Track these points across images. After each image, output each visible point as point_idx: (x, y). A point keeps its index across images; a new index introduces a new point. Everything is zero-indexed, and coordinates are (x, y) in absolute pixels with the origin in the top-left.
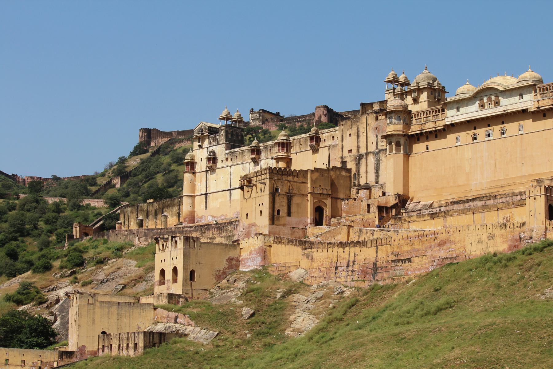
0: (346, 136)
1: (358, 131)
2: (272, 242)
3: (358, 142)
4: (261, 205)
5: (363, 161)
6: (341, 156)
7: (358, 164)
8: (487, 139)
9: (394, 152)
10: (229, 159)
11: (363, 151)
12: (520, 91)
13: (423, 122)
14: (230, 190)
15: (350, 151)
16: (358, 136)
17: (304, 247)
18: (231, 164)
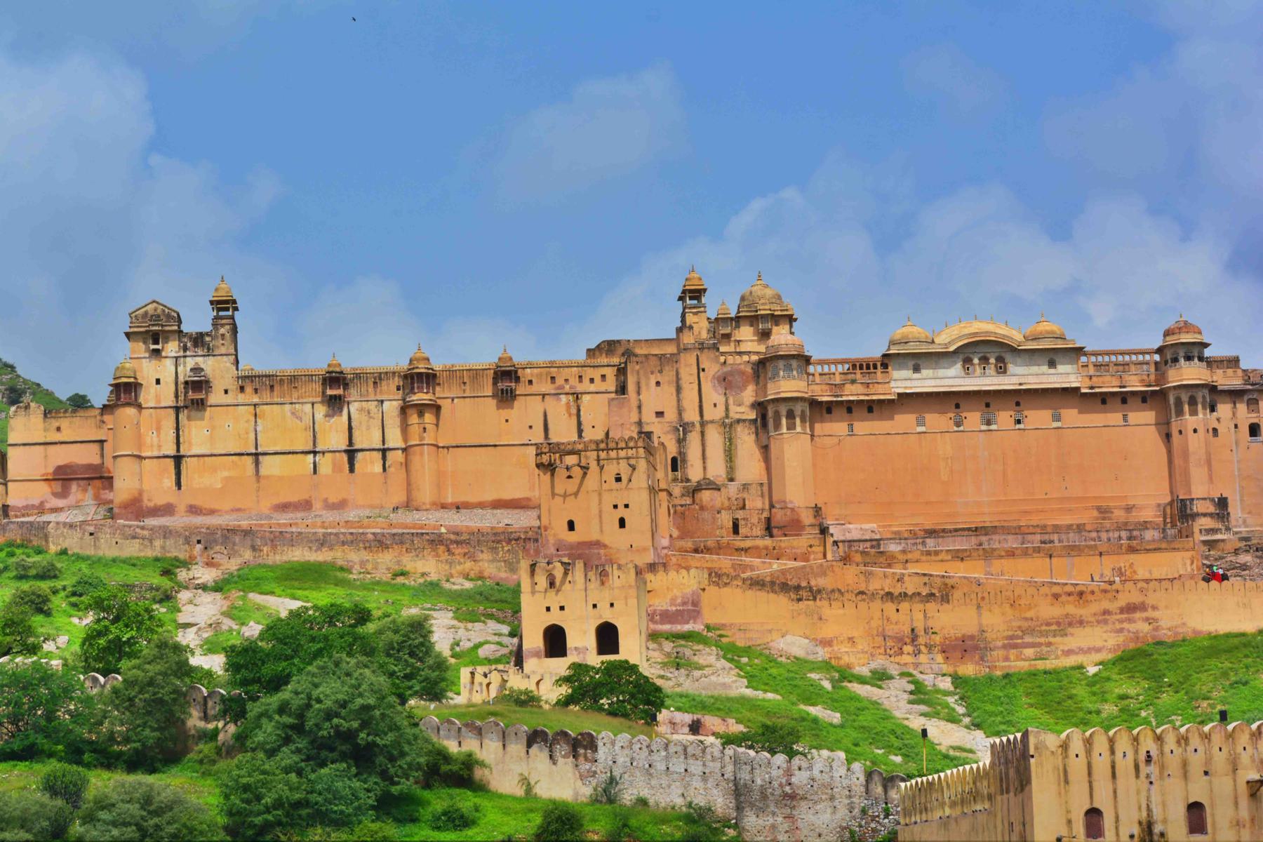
0: (647, 385)
1: (678, 379)
2: (706, 582)
3: (679, 400)
4: (621, 507)
5: (694, 439)
6: (636, 420)
7: (681, 442)
8: (984, 427)
9: (799, 429)
10: (249, 389)
11: (691, 415)
12: (1052, 355)
13: (838, 382)
14: (256, 455)
15: (660, 414)
16: (679, 390)
17: (793, 596)
18: (256, 400)
